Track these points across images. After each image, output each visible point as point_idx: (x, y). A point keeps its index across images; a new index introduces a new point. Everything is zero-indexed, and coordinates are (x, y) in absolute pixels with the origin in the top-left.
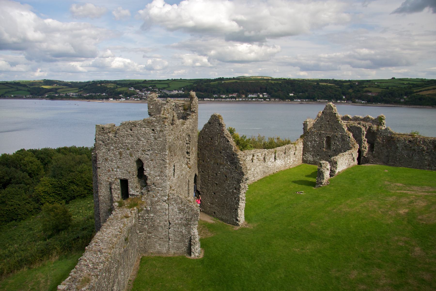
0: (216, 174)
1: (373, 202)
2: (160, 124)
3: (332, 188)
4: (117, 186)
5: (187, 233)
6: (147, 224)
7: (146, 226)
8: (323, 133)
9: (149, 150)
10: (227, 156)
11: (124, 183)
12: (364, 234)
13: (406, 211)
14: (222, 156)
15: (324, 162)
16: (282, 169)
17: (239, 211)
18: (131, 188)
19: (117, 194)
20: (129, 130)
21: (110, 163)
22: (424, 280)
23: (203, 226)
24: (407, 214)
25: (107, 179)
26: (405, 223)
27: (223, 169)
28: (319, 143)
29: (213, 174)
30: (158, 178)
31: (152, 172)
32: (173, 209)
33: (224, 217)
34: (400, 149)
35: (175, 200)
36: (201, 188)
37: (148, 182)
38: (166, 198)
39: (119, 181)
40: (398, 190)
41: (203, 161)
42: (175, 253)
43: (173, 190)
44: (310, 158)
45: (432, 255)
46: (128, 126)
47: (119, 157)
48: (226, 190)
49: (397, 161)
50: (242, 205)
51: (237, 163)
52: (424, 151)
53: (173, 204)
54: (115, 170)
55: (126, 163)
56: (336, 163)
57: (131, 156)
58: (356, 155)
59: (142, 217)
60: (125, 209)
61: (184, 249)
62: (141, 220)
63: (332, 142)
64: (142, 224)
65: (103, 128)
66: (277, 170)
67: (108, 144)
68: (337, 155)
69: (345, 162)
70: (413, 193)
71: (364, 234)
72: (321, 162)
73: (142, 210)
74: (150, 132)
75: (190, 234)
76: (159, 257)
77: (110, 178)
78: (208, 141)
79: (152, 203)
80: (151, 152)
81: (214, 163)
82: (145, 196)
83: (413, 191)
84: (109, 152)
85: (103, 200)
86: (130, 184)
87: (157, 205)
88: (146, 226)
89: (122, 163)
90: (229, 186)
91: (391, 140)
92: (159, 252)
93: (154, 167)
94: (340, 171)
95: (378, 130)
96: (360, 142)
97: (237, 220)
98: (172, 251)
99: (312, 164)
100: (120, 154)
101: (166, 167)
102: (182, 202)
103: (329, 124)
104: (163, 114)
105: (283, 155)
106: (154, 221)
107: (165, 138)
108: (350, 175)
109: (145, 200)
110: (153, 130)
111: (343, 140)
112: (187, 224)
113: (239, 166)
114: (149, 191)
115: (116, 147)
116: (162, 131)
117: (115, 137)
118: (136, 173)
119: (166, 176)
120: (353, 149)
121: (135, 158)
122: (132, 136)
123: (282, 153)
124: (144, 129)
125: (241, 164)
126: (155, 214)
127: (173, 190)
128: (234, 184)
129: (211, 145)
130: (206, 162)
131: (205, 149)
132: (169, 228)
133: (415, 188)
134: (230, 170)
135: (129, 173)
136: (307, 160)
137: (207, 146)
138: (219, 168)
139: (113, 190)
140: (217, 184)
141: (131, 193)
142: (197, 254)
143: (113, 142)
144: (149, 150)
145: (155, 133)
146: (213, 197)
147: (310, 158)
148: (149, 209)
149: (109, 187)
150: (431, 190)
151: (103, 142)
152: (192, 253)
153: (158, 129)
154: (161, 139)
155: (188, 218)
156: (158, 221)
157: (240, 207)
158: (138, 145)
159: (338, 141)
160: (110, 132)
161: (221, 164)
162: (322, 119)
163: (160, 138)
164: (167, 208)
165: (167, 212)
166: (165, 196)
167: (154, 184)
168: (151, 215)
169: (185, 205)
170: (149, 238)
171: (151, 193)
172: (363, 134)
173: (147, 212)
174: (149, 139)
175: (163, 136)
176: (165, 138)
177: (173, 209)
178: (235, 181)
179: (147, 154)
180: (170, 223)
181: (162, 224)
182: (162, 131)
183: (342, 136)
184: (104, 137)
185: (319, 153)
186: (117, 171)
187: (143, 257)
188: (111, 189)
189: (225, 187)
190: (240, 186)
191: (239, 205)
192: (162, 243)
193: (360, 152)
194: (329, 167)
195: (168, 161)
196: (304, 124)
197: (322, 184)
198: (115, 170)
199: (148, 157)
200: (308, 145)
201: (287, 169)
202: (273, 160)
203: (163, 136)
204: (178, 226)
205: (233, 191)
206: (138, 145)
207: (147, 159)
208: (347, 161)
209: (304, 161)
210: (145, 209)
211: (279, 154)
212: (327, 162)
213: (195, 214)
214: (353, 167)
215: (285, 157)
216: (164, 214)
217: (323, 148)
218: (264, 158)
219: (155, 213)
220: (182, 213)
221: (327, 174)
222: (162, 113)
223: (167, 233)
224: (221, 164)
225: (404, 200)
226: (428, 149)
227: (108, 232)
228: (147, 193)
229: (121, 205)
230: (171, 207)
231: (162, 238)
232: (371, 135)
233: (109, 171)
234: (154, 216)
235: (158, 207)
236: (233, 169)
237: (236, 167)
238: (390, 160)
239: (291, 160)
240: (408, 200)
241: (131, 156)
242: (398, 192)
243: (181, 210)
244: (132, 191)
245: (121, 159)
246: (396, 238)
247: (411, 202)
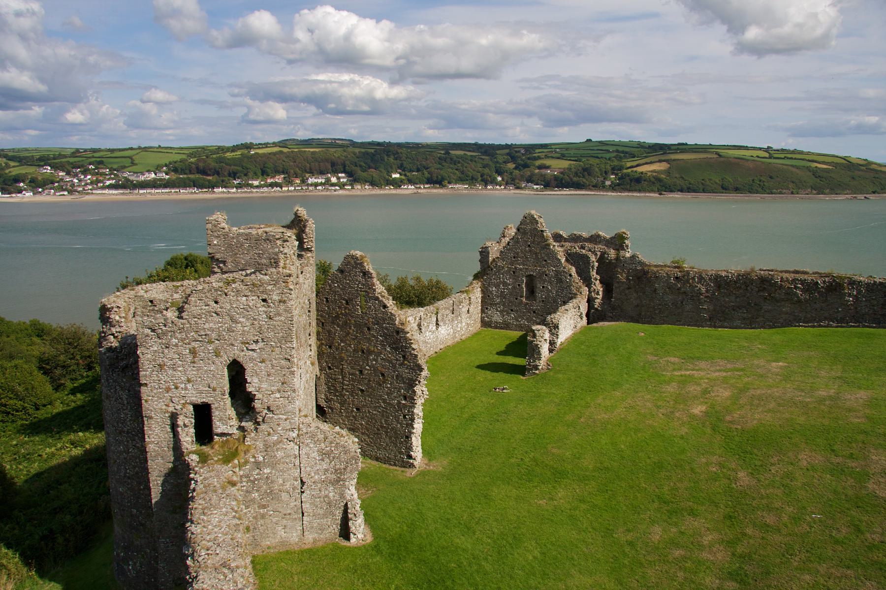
0: (361, 372)
1: (643, 397)
2: (279, 289)
3: (560, 376)
4: (187, 420)
5: (337, 497)
6: (257, 491)
7: (255, 495)
8: (521, 269)
9: (257, 342)
10: (385, 335)
11: (203, 413)
12: (649, 458)
13: (704, 408)
14: (374, 336)
15: (539, 327)
16: (450, 343)
17: (413, 438)
18: (220, 420)
19: (188, 437)
20: (212, 304)
21: (170, 372)
22: (768, 526)
23: (363, 480)
24: (706, 414)
25: (164, 407)
26: (709, 430)
27: (374, 360)
28: (514, 287)
29: (352, 371)
30: (278, 395)
31: (264, 386)
32: (308, 455)
33: (381, 454)
34: (660, 292)
35: (313, 436)
36: (328, 400)
37: (257, 405)
38: (295, 435)
39: (191, 408)
40: (674, 370)
41: (330, 347)
42: (315, 541)
43: (306, 416)
44: (497, 317)
45: (767, 482)
46: (208, 295)
47: (190, 358)
48: (384, 401)
50: (418, 426)
51: (406, 347)
52: (701, 294)
53: (307, 445)
54: (183, 386)
55: (206, 371)
56: (556, 327)
57: (217, 355)
58: (584, 308)
59: (247, 476)
60: (218, 467)
61: (336, 528)
62: (244, 484)
63: (538, 285)
64: (247, 492)
65: (151, 301)
66: (442, 347)
67: (164, 334)
68: (555, 312)
69: (570, 321)
70: (702, 374)
71: (649, 458)
72: (534, 328)
73: (246, 462)
74: (258, 305)
75: (344, 498)
76: (287, 552)
77: (171, 404)
78: (339, 307)
79: (267, 447)
80: (261, 344)
81: (354, 350)
82: (253, 435)
83: (701, 370)
84: (166, 351)
85: (155, 451)
86: (216, 414)
87: (277, 450)
88: (255, 495)
89: (198, 370)
90: (388, 394)
91: (642, 276)
92: (283, 543)
93: (269, 375)
94: (563, 340)
95: (617, 258)
96: (588, 282)
97: (410, 457)
98: (310, 537)
99: (501, 328)
100: (193, 352)
101: (293, 373)
102: (326, 438)
103: (530, 251)
104: (284, 268)
105: (451, 316)
106: (272, 482)
107: (289, 315)
108: (583, 347)
109: (253, 442)
110: (264, 300)
111: (560, 281)
112: (338, 481)
113: (411, 354)
114: (258, 423)
115: (182, 340)
116: (284, 302)
117: (180, 317)
118: (227, 388)
119: (294, 391)
120: (579, 298)
121: (226, 359)
122: (218, 314)
123: (448, 312)
124: (244, 298)
125: (414, 349)
126: (273, 468)
127: (306, 416)
128: (401, 388)
129: (346, 315)
130: (337, 349)
131: (333, 323)
132: (303, 492)
133: (702, 364)
134: (390, 362)
135: (214, 390)
136: (491, 321)
137: (337, 317)
138: (368, 359)
139: (179, 429)
140: (362, 391)
141: (219, 431)
142: (360, 536)
143: (175, 328)
144: (257, 342)
145: (269, 307)
146: (353, 417)
147: (497, 317)
148: (261, 459)
149: (169, 422)
150: (729, 366)
151: (153, 331)
152: (352, 535)
153: (276, 297)
154: (283, 318)
155: (340, 469)
156: (281, 481)
157: (414, 431)
158: (233, 331)
159: (550, 283)
160: (167, 309)
161: (370, 352)
162: (518, 242)
163: (280, 315)
164: (297, 453)
165: (297, 463)
166: (292, 430)
167: (269, 408)
168: (265, 471)
169: (331, 443)
170: (263, 516)
171: (263, 427)
172: (593, 267)
173: (258, 465)
174: (255, 319)
175: (285, 311)
176: (289, 315)
177: (308, 455)
178: (404, 383)
179: (253, 350)
180: (303, 483)
181: (288, 486)
182: (284, 302)
183: (557, 273)
184: (156, 319)
186: (186, 389)
187: (254, 556)
188: (174, 427)
189: (381, 396)
190: (415, 392)
191: (413, 428)
192: (289, 523)
193: (590, 301)
194: (547, 335)
195: (296, 360)
196: (481, 252)
197: (537, 369)
198: (183, 386)
199: (255, 354)
201: (458, 343)
202: (434, 328)
203: (285, 311)
204: (319, 485)
205: (399, 403)
206: (233, 331)
207: (252, 359)
208: (572, 322)
209: (485, 324)
210: (253, 460)
211: (443, 315)
212: (544, 327)
213: (353, 458)
214: (583, 331)
216: (291, 465)
217: (522, 297)
218: (419, 325)
219: (273, 466)
220: (327, 460)
221: (545, 349)
222: (281, 264)
223: (298, 503)
224: (370, 352)
225: (693, 389)
226: (707, 291)
227: (215, 521)
228: (256, 429)
229: (204, 459)
230: (303, 452)
231: (290, 514)
232: (607, 269)
233: (168, 390)
234: (271, 473)
235: (280, 454)
236: (397, 360)
237: (404, 357)
240: (699, 388)
241: (217, 355)
242: (679, 373)
243: (325, 455)
244: (219, 427)
245: (194, 362)
246: (704, 460)
247: (705, 392)
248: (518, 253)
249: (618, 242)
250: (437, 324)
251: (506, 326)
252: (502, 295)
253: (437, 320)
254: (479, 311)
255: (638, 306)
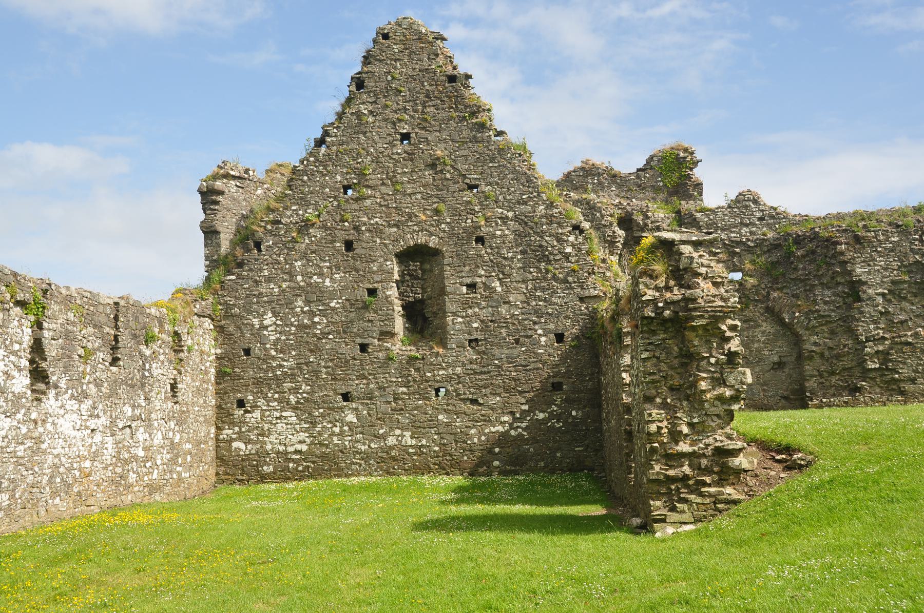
8: (376, 230)
49: (866, 373)
103: (411, 156)
136: (262, 455)
147: (288, 435)
159: (499, 268)
185: (356, 386)
196: (209, 197)
200: (258, 334)
202: (21, 382)
209: (238, 470)
215: (113, 394)
238: (811, 384)
239: (158, 439)
248: (361, 175)
249: (673, 174)
250: (38, 375)
251: (323, 464)
252: (306, 341)
253: (37, 347)
254: (210, 413)
255: (779, 365)
